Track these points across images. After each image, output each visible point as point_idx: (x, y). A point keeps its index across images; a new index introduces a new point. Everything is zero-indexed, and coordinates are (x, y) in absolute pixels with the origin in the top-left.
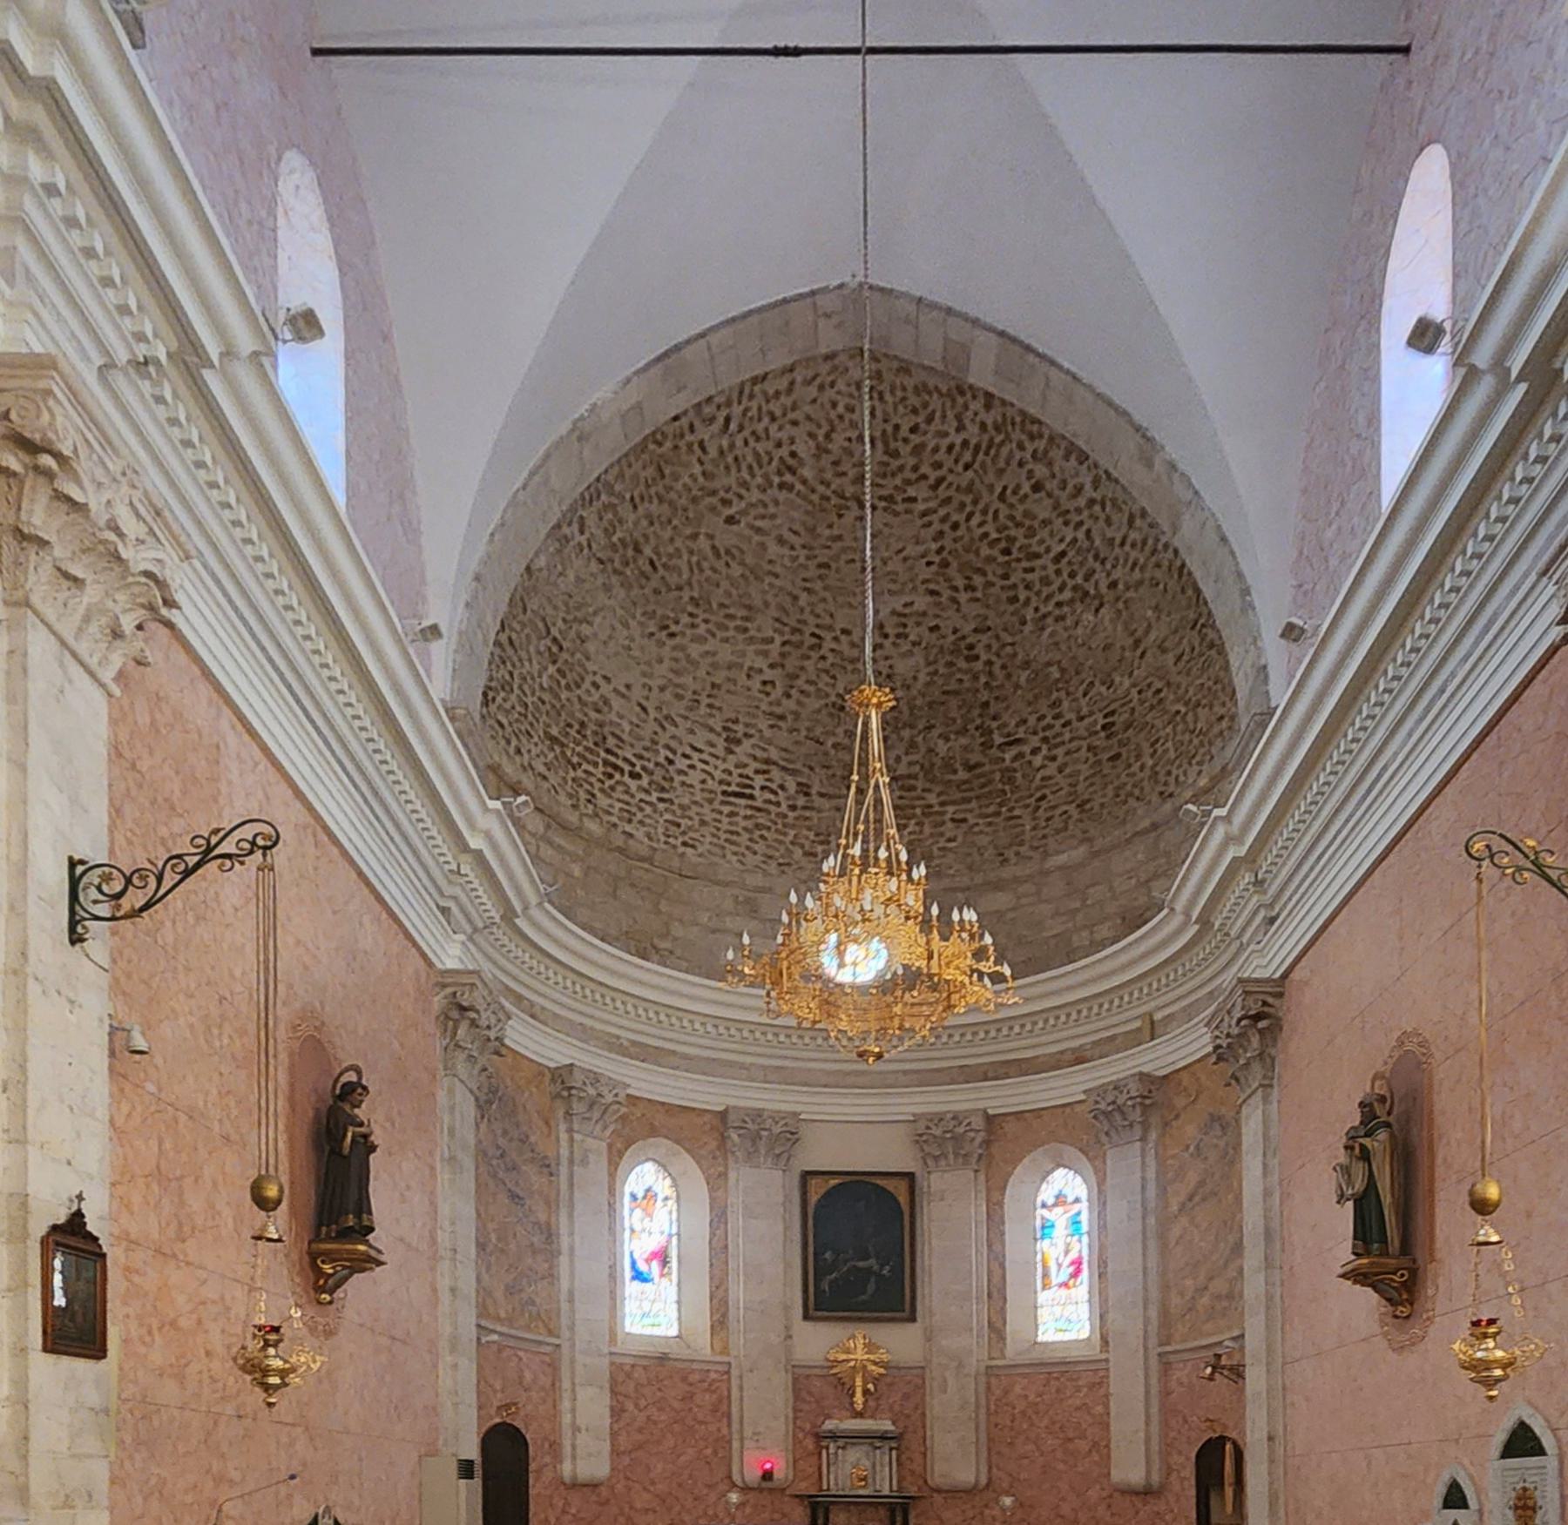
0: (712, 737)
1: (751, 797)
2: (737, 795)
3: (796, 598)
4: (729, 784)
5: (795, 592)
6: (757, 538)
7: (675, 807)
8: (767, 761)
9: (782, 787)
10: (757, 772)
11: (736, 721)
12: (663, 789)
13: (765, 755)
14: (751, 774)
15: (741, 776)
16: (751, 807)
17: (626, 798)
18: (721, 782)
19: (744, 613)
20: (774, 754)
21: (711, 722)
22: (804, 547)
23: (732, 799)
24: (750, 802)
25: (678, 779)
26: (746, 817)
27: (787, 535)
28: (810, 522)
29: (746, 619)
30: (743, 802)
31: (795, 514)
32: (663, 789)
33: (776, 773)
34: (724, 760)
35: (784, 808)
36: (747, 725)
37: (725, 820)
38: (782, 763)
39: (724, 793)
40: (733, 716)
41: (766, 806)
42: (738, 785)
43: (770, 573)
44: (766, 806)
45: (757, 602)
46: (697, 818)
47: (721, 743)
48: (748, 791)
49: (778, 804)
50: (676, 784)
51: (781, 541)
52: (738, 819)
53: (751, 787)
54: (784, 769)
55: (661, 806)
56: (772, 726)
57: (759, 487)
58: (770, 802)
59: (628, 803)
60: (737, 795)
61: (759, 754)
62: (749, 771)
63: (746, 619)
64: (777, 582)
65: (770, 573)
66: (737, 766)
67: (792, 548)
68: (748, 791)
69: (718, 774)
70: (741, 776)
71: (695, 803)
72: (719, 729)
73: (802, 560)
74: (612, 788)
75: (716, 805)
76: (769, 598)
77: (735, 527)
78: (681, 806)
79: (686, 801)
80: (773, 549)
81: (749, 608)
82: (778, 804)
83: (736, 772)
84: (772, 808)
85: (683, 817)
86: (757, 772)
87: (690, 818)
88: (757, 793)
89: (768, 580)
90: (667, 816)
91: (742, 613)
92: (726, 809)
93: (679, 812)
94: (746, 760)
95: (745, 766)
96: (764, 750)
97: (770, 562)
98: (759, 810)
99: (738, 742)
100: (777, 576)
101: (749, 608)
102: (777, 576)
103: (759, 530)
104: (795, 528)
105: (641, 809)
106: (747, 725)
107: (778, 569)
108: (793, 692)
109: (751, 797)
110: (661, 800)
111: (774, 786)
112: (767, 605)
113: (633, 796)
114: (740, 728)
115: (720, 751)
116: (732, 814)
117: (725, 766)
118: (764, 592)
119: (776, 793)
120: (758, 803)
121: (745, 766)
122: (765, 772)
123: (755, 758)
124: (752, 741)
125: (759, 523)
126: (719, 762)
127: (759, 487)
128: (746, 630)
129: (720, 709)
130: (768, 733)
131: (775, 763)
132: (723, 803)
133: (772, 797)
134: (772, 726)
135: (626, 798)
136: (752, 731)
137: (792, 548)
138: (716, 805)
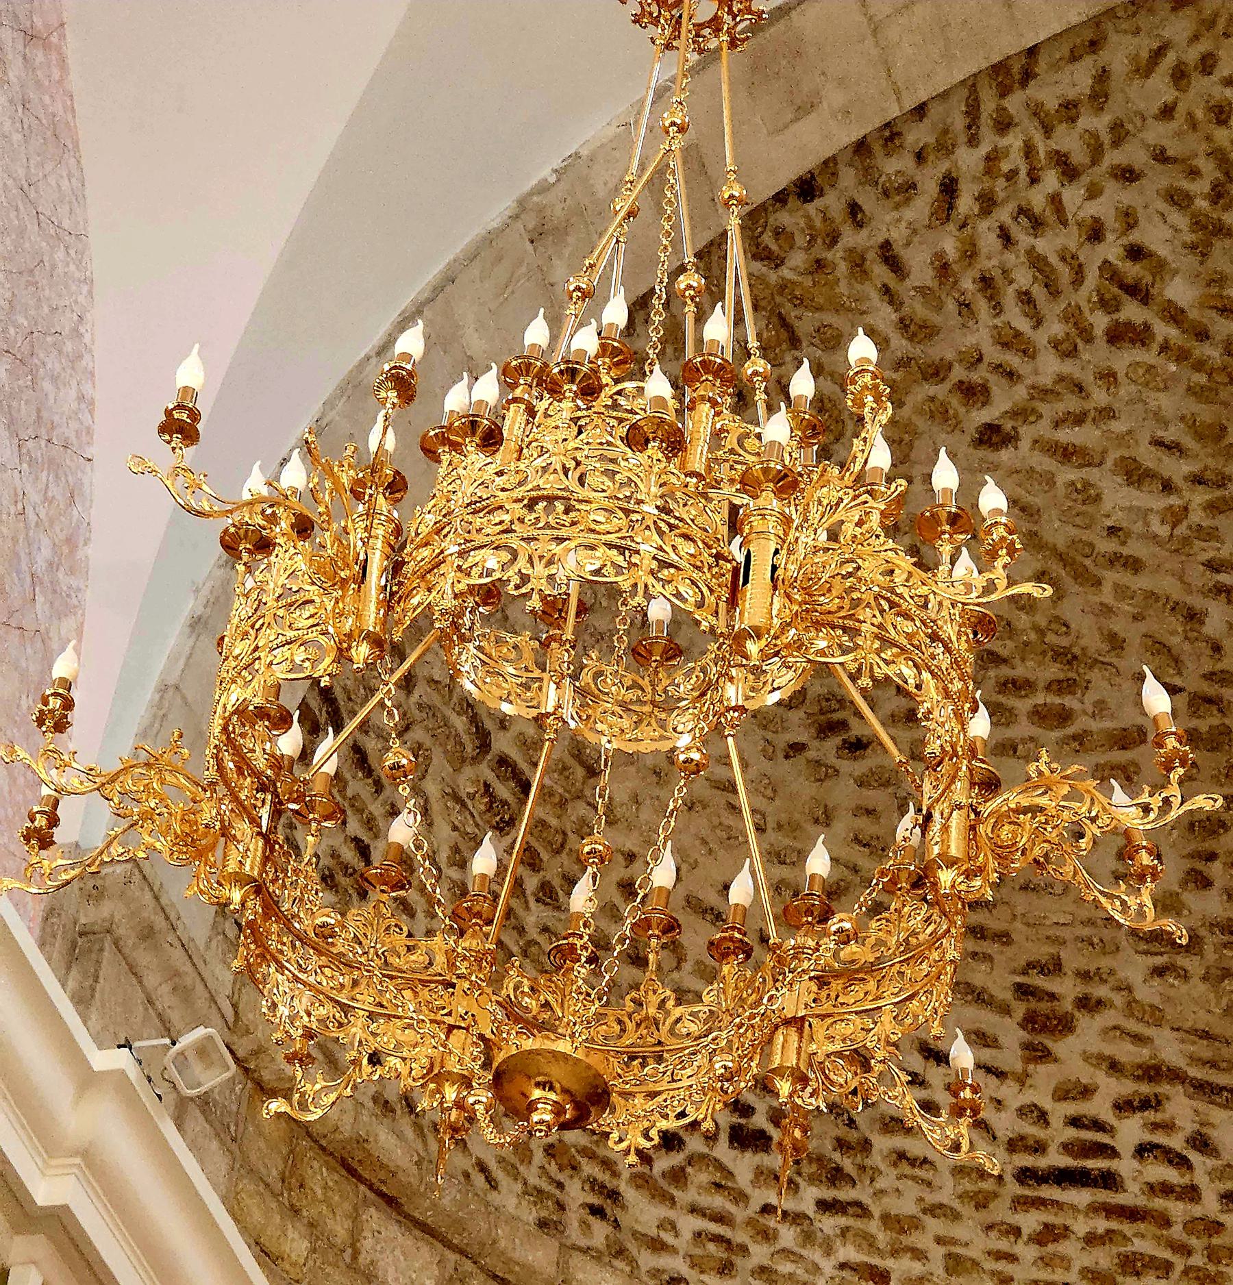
0: (987, 1019)
1: (1109, 1180)
2: (1064, 1177)
3: (1193, 617)
4: (1039, 1148)
5: (1197, 602)
6: (1067, 475)
7: (874, 1226)
8: (1152, 1072)
9: (1201, 1143)
10: (1124, 1106)
11: (1054, 967)
12: (836, 1176)
13: (1143, 1054)
14: (1107, 1116)
15: (1075, 1122)
16: (1111, 1211)
17: (718, 1202)
18: (1015, 1145)
19: (1054, 671)
20: (1170, 1049)
21: (979, 976)
22: (1198, 480)
23: (1050, 1192)
24: (1103, 1196)
25: (883, 1143)
26: (1091, 1240)
27: (1148, 457)
28: (1206, 413)
29: (1062, 686)
30: (1081, 1197)
31: (1166, 402)
32: (836, 1176)
33: (1181, 1107)
34: (1022, 1080)
35: (1210, 1205)
36: (1085, 976)
37: (1027, 1252)
38: (1194, 1072)
39: (1025, 1175)
40: (1043, 952)
41: (1159, 1203)
42: (1067, 1148)
43: (1114, 560)
44: (1159, 1203)
45: (1092, 642)
46: (937, 1252)
47: (1011, 1034)
48: (1095, 1164)
49: (1191, 1193)
50: (876, 1159)
51: (1135, 474)
52: (1068, 1248)
53: (1112, 1152)
54: (1203, 1089)
55: (829, 1224)
56: (1159, 972)
57: (1055, 344)
58: (1166, 1189)
59: (720, 1218)
60: (1064, 1177)
61: (1127, 1052)
62: (1100, 1107)
63: (1062, 686)
64: (1142, 582)
65: (1114, 560)
66: (1063, 1094)
67: (1168, 487)
68: (1095, 1164)
69: (1006, 1124)
70: (1075, 1122)
71: (934, 1210)
72: (1008, 996)
73: (1197, 516)
74: (677, 1176)
75: (1001, 1211)
76: (1118, 625)
77: (1005, 455)
78: (888, 1220)
79: (907, 1206)
80: (1118, 498)
81: (1064, 656)
82: (1191, 1193)
83: (1059, 1111)
84: (1177, 1209)
85: (895, 1253)
86: (1124, 1106)
87: (919, 1254)
88: (1125, 1166)
89: (1111, 577)
90: (849, 1252)
91: (1054, 671)
92: (1030, 1221)
93: (883, 1238)
94: (1086, 1074)
95: (1086, 1092)
96: (1138, 1039)
97: (1113, 531)
98: (1132, 1214)
99: (1065, 1025)
100: (1134, 565)
101: (1064, 656)
102: (1134, 565)
103: (1067, 453)
104: (1169, 435)
105: (767, 1236)
106: (1085, 976)
107: (1134, 548)
108: (1216, 869)
109: (1109, 1180)
110: (825, 1206)
111: (1176, 1142)
112: (1116, 643)
113: (740, 1197)
114: (1067, 988)
115: (1010, 1057)
116: (1048, 1234)
117: (1028, 1097)
118: (1106, 610)
119: (1182, 1162)
120: (1132, 1196)
121: (1086, 1092)
122: (1145, 1104)
123: (1114, 1066)
124: (1107, 1018)
125: (1066, 435)
126: (1008, 1091)
127: (1055, 344)
128: (1064, 717)
129: (1004, 938)
130: (1148, 992)
131: (1176, 1076)
132: (1021, 1203)
133: (1172, 1175)
134: (1159, 972)
135: (718, 1202)
136: (1101, 991)
137: (1168, 487)
138: (1001, 1211)
